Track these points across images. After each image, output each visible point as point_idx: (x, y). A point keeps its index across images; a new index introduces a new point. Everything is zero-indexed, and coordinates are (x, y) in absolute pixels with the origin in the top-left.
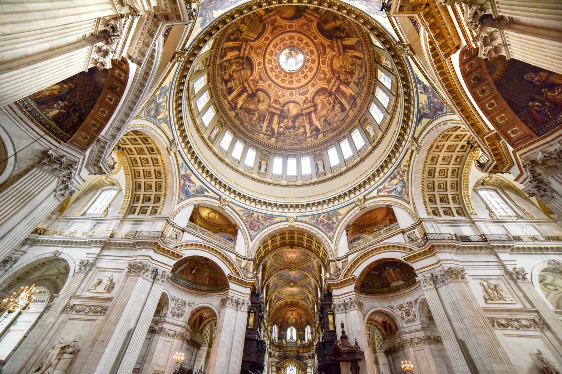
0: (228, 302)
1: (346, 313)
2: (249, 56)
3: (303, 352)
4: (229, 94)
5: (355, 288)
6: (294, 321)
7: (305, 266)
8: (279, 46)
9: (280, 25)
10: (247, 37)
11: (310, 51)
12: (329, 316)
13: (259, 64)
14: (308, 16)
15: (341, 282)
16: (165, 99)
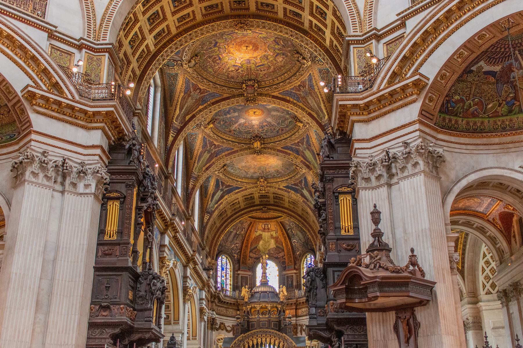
0: (29, 170)
1: (390, 185)
3: (297, 316)
5: (421, 114)
6: (272, 244)
7: (288, 88)
12: (341, 198)
15: (379, 100)
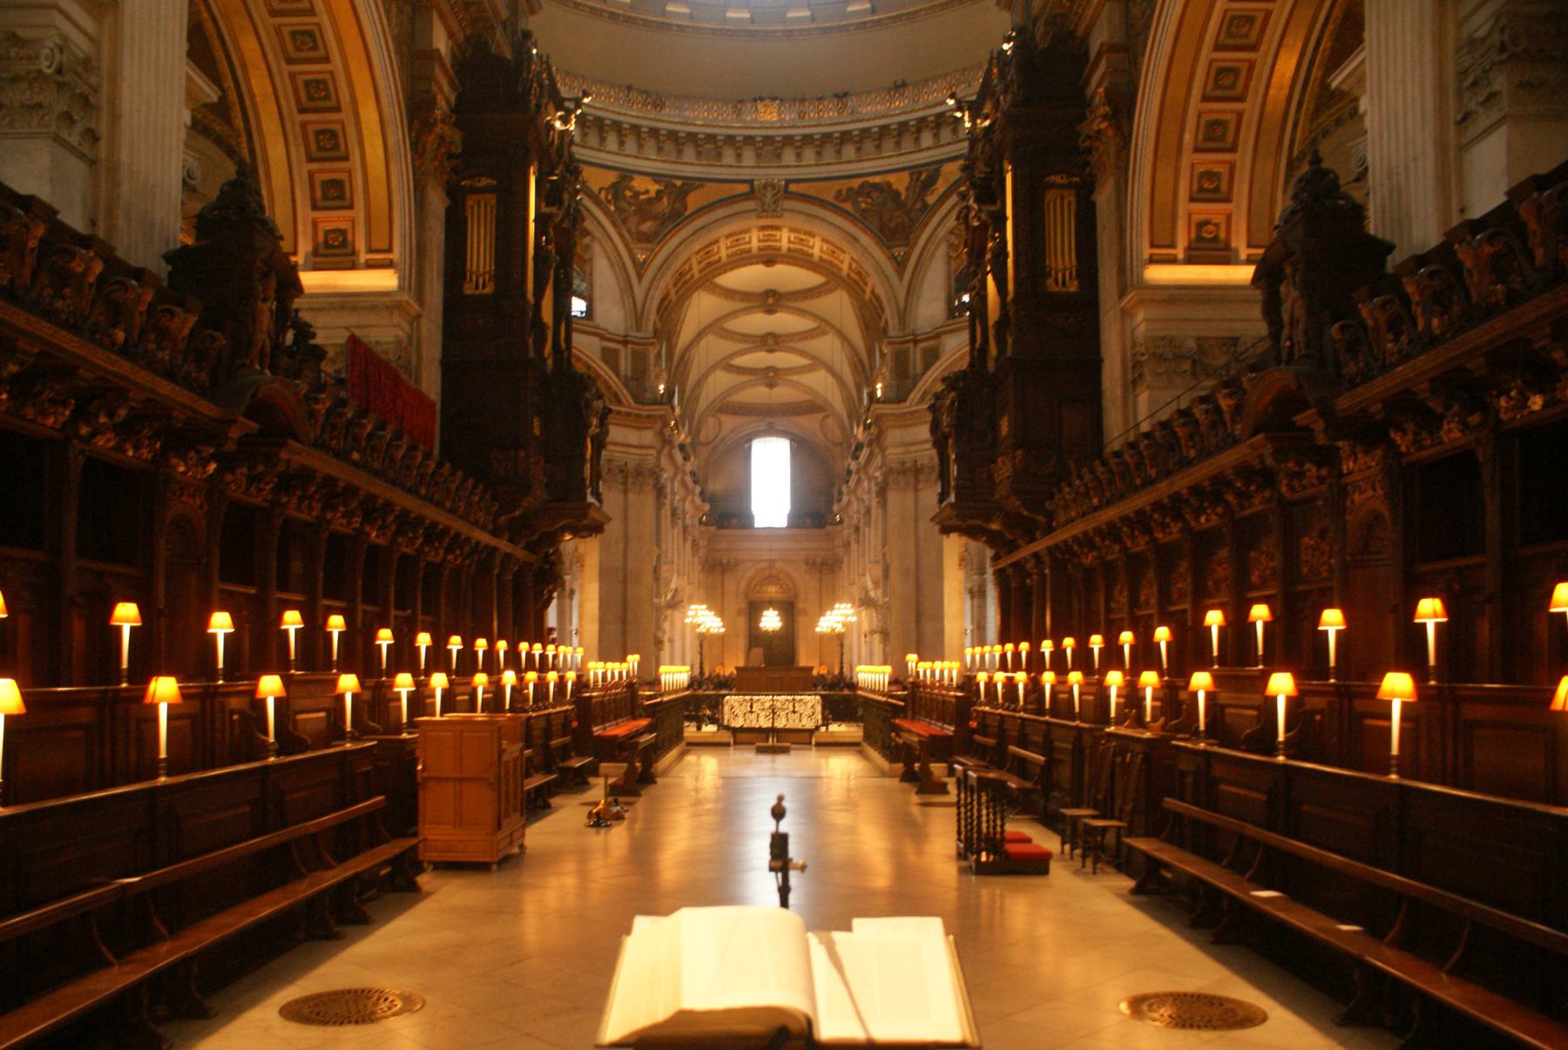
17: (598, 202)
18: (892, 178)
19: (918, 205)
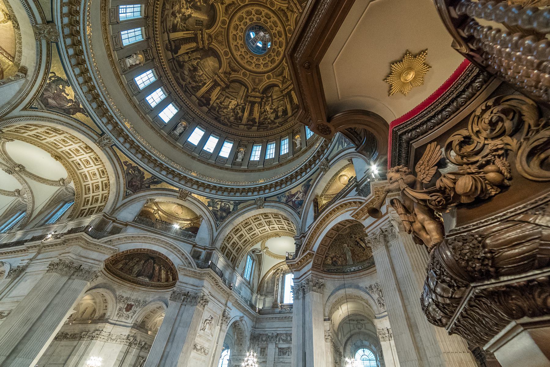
2: (261, 91)
4: (287, 114)
8: (249, 60)
9: (228, 65)
10: (244, 97)
11: (241, 22)
13: (269, 78)
14: (207, 42)
16: (220, 203)
17: (46, 73)
18: (146, 172)
19: (147, 185)
